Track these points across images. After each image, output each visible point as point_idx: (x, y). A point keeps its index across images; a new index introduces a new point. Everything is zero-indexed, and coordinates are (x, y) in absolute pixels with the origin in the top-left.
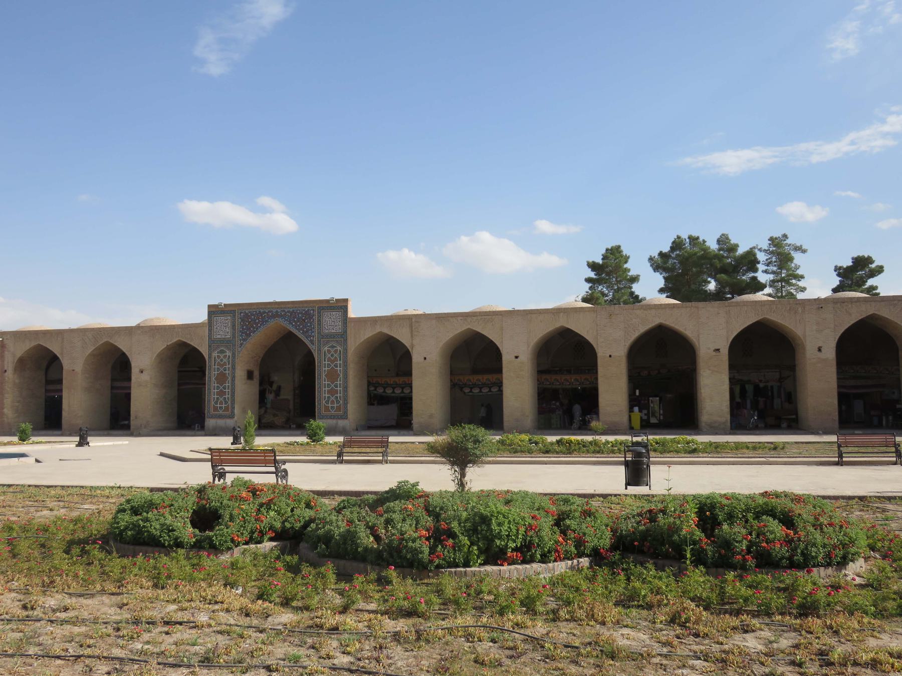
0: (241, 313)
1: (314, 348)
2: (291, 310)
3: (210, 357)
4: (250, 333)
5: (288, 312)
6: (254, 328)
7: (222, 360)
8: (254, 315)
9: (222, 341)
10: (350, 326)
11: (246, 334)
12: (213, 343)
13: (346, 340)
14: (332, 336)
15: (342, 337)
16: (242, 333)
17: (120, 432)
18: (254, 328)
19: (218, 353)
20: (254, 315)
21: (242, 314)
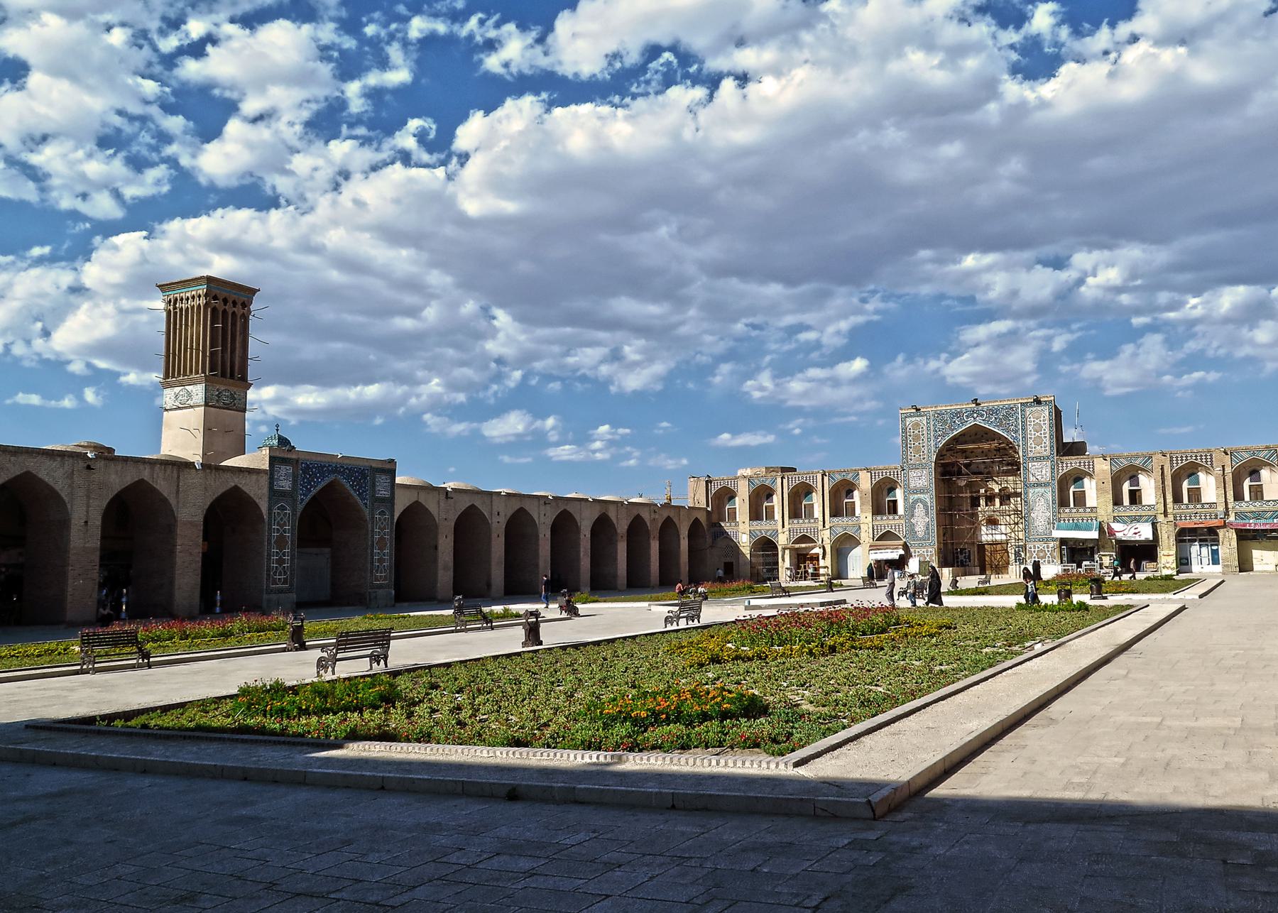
0: (302, 463)
1: (367, 511)
2: (350, 467)
3: (270, 514)
4: (310, 488)
5: (347, 468)
6: (315, 482)
7: (282, 519)
8: (315, 468)
9: (283, 494)
10: (398, 492)
11: (306, 487)
12: (275, 495)
13: (393, 505)
14: (383, 500)
15: (390, 501)
16: (303, 487)
17: (519, 596)
18: (315, 482)
19: (278, 508)
20: (315, 468)
21: (303, 465)
